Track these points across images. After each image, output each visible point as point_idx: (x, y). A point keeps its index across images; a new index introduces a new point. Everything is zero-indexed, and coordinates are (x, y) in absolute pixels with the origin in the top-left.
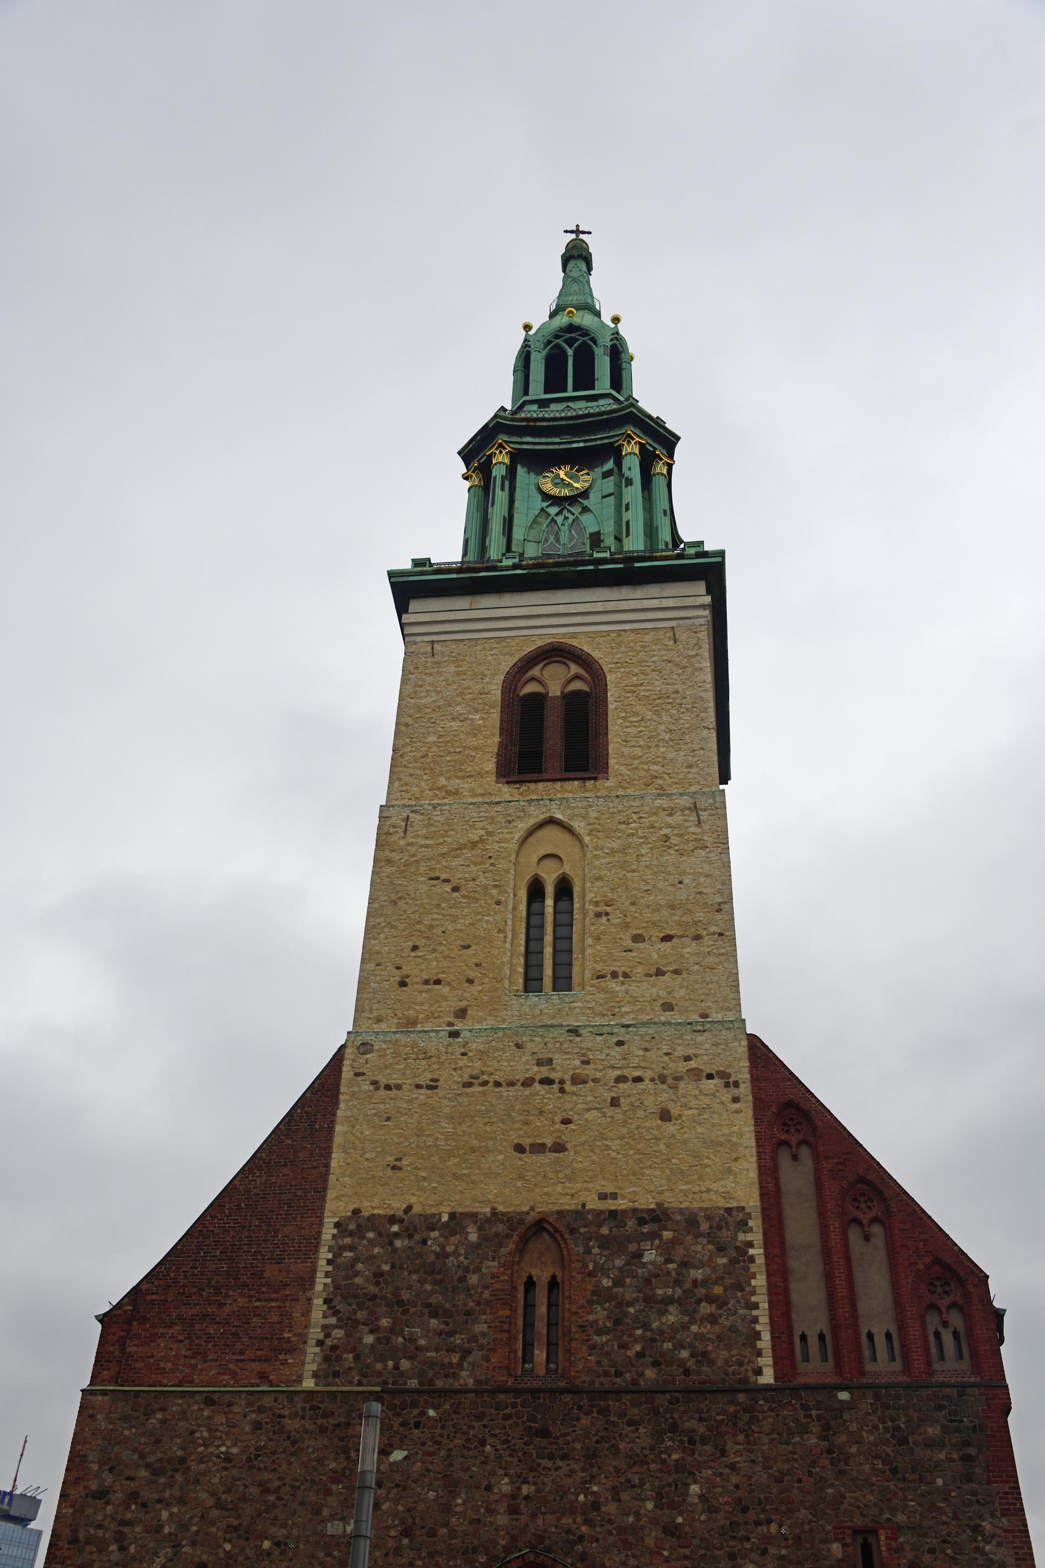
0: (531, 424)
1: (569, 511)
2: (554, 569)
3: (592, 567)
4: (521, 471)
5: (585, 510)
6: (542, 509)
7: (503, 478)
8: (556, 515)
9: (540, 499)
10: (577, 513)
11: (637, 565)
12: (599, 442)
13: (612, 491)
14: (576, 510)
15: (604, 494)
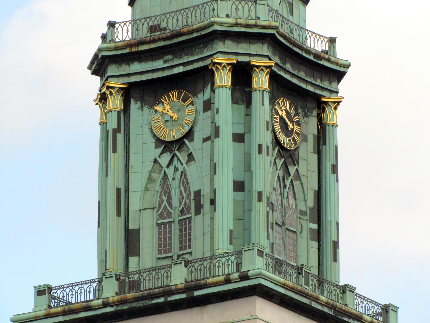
0: (134, 50)
1: (178, 159)
2: (135, 305)
3: (162, 300)
4: (134, 106)
5: (191, 157)
6: (156, 161)
7: (116, 131)
8: (168, 167)
9: (153, 145)
10: (184, 162)
11: (197, 293)
12: (196, 66)
13: (209, 135)
14: (182, 156)
15: (205, 137)
